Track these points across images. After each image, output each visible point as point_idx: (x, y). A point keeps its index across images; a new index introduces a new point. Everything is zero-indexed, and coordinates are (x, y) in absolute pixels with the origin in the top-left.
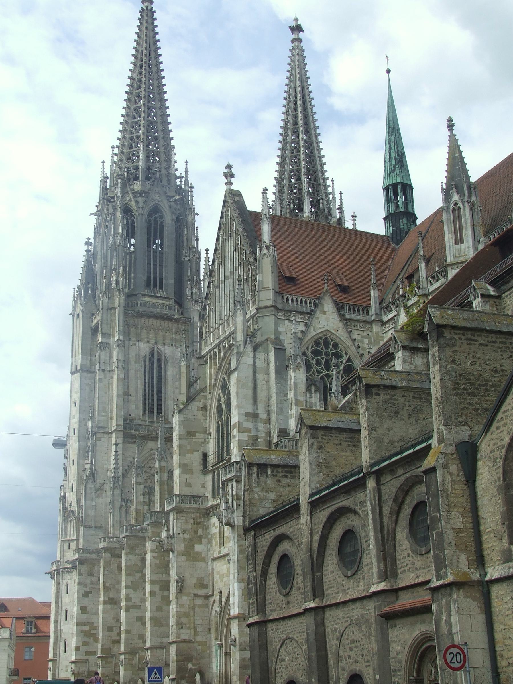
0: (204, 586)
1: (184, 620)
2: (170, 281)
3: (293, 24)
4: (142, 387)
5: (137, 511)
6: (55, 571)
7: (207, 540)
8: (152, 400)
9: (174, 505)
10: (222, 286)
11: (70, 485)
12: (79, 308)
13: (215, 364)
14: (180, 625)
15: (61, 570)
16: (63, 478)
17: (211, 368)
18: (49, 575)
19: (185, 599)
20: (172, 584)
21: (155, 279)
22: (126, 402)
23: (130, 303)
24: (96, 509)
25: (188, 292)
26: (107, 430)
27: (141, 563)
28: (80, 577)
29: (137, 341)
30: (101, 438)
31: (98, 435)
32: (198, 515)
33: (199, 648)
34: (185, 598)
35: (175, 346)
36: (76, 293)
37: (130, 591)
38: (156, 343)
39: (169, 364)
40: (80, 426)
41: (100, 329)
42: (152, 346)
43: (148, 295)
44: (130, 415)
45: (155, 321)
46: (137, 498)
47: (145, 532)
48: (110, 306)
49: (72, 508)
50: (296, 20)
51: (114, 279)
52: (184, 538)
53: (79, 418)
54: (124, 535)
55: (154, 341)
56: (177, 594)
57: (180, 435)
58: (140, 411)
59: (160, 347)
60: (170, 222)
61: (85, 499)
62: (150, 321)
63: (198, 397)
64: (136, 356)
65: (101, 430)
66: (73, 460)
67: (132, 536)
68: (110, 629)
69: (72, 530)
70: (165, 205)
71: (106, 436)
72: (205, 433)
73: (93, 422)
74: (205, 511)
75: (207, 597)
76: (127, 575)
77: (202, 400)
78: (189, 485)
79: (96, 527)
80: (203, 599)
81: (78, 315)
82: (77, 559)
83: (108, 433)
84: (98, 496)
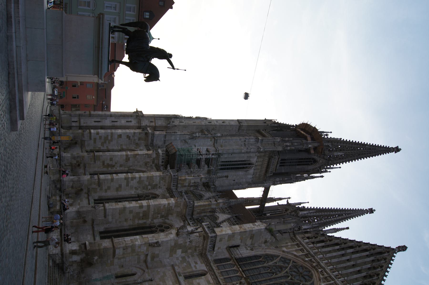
0: (153, 258)
1: (129, 250)
2: (283, 170)
3: (373, 209)
4: (235, 160)
5: (186, 179)
6: (138, 113)
7: (184, 255)
8: (228, 165)
9: (210, 235)
10: (343, 252)
11: (183, 121)
12: (269, 123)
13: (296, 251)
14: (126, 248)
15: (139, 118)
16: (186, 116)
17: (291, 245)
18: (135, 111)
19: (144, 249)
20: (153, 237)
21: (284, 163)
22: (229, 154)
23: (275, 152)
24: (175, 140)
25: (278, 179)
26: (215, 144)
27: (154, 185)
28: (138, 133)
29: (258, 157)
30: (212, 141)
31: (213, 140)
32: (201, 248)
33: (109, 261)
34: (145, 248)
35: (254, 175)
36: (274, 121)
37: (138, 180)
38: (256, 166)
39: (245, 172)
40: (212, 125)
41: (264, 138)
42: (254, 164)
43: (278, 160)
44: (222, 155)
45: (266, 164)
46: (193, 179)
47: (180, 198)
48: (275, 143)
49: (171, 122)
50: (375, 210)
51: (288, 144)
52: (186, 243)
53: (217, 125)
54: (172, 173)
55: (256, 164)
56: (148, 243)
57: (252, 231)
58: (223, 160)
59: (253, 168)
60: (309, 168)
61: (180, 134)
62: (266, 162)
63: (273, 237)
64: (250, 157)
65: (216, 141)
66: (195, 122)
67: (171, 178)
68: (111, 159)
69: (160, 123)
70: (317, 166)
71: (212, 144)
72: (251, 244)
73: (219, 137)
74: (203, 252)
75: (145, 261)
76: (148, 177)
77: (271, 240)
78: (221, 240)
79: (165, 141)
80: (144, 259)
81: (265, 123)
82: (148, 131)
83: (214, 144)
84: (181, 141)
